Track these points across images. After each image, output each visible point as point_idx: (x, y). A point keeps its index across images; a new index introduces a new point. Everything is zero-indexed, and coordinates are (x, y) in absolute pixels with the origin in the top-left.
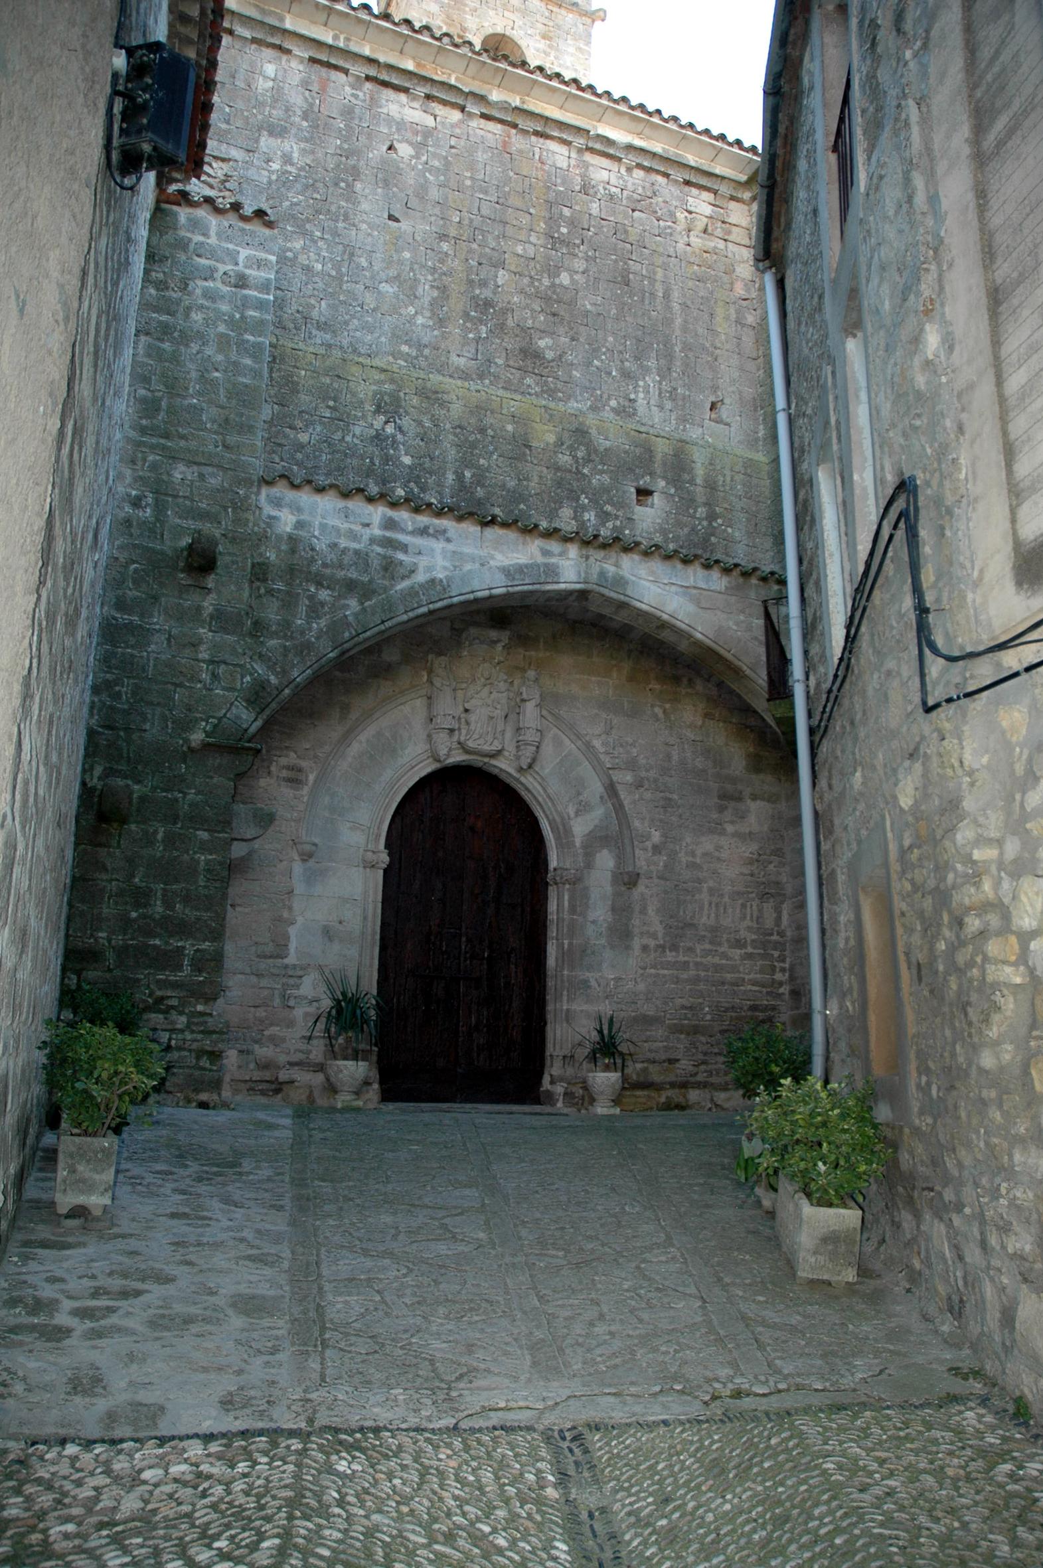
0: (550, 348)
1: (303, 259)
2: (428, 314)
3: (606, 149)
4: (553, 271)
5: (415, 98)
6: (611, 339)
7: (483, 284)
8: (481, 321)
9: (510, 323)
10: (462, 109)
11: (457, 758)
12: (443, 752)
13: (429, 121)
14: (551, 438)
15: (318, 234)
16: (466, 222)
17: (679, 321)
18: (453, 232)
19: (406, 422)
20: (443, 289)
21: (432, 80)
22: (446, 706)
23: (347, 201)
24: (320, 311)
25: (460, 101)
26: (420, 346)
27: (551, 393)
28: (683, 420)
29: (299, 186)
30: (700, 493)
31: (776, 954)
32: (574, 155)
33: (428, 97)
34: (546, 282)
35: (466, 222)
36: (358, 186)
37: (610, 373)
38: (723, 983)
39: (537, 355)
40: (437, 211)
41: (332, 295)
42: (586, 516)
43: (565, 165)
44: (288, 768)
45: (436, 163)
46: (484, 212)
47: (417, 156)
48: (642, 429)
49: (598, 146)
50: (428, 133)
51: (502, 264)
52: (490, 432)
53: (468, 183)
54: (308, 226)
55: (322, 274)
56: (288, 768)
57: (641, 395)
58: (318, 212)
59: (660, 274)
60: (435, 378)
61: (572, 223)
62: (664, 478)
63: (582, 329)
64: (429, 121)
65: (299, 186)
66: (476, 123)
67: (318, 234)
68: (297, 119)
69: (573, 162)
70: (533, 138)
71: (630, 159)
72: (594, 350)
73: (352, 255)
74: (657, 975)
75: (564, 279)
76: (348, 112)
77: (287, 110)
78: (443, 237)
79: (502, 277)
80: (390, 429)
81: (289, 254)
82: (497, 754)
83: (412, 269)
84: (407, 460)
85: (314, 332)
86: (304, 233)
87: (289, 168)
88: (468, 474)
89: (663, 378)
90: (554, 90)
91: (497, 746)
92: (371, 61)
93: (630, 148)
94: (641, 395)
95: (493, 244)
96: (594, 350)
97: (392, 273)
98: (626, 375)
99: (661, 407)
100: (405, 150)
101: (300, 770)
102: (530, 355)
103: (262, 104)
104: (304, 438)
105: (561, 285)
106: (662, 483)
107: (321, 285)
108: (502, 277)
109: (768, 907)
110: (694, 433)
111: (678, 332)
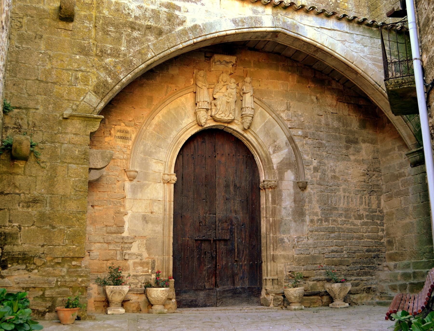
11: (211, 124)
12: (203, 121)
22: (204, 96)
31: (379, 222)
38: (352, 238)
44: (120, 131)
56: (120, 131)
91: (231, 117)
101: (127, 132)
109: (373, 197)
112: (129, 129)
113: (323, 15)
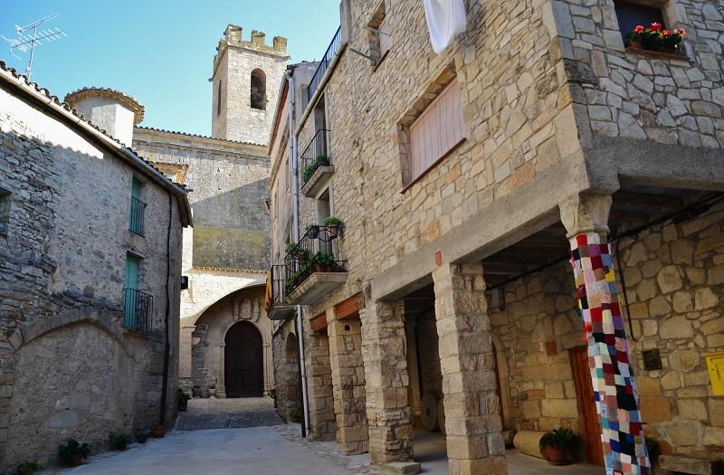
19: (225, 242)
27: (260, 228)
39: (256, 219)
100: (221, 170)
102: (254, 219)
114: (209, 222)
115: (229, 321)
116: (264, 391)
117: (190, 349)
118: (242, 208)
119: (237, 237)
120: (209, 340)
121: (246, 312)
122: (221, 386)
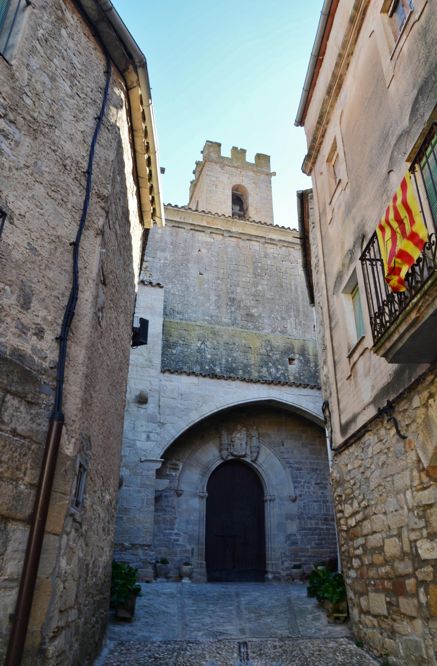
0: (256, 312)
1: (172, 291)
2: (214, 305)
3: (272, 242)
4: (256, 285)
5: (207, 233)
6: (277, 307)
7: (232, 293)
8: (232, 306)
9: (242, 305)
10: (223, 235)
11: (230, 458)
12: (224, 457)
13: (212, 240)
14: (258, 344)
15: (177, 282)
16: (226, 272)
17: (301, 298)
18: (221, 276)
19: (208, 343)
20: (219, 296)
21: (212, 228)
23: (186, 270)
24: (178, 308)
25: (222, 233)
26: (212, 316)
27: (257, 328)
28: (304, 332)
29: (170, 267)
30: (312, 358)
32: (261, 245)
33: (211, 233)
34: (254, 289)
35: (226, 272)
36: (189, 265)
37: (277, 319)
40: (216, 270)
41: (182, 302)
42: (271, 370)
43: (258, 249)
45: (215, 254)
46: (231, 268)
47: (208, 252)
48: (290, 337)
49: (269, 241)
50: (211, 244)
51: (238, 285)
52: (237, 344)
53: (226, 259)
54: (173, 280)
55: (178, 295)
56: (172, 464)
57: (289, 325)
58: (176, 275)
59: (293, 283)
60: (217, 327)
61: (262, 268)
62: (299, 354)
63: (267, 304)
64: (212, 240)
65: (170, 267)
66: (227, 239)
67: (177, 282)
68: (169, 246)
69: (261, 248)
70: (247, 241)
71: (281, 244)
72: (272, 311)
73: (188, 288)
74: (305, 533)
75: (260, 288)
76: (185, 241)
77: (166, 243)
78: (218, 278)
79: (239, 290)
80: (203, 346)
81: (167, 290)
82: (244, 456)
83: (208, 290)
84: (209, 356)
85: (176, 315)
86: (172, 282)
87: (166, 262)
88: (230, 359)
89: (296, 318)
90: (253, 225)
91: (243, 453)
92: (192, 224)
93: (280, 241)
94: (289, 325)
95: (235, 279)
96: (272, 311)
97: (201, 292)
98: (283, 319)
99: (296, 329)
100: (204, 251)
101: (177, 465)
102: (249, 315)
103: (157, 242)
104: (174, 351)
105: (259, 290)
106: (298, 356)
107: (178, 299)
108: (239, 290)
110: (308, 336)
111: (301, 302)
112: (178, 463)
113: (301, 387)
114: (186, 316)
115: (210, 455)
116: (267, 572)
117: (152, 496)
118: (232, 300)
119: (226, 338)
120: (183, 487)
121: (241, 442)
122: (198, 562)
